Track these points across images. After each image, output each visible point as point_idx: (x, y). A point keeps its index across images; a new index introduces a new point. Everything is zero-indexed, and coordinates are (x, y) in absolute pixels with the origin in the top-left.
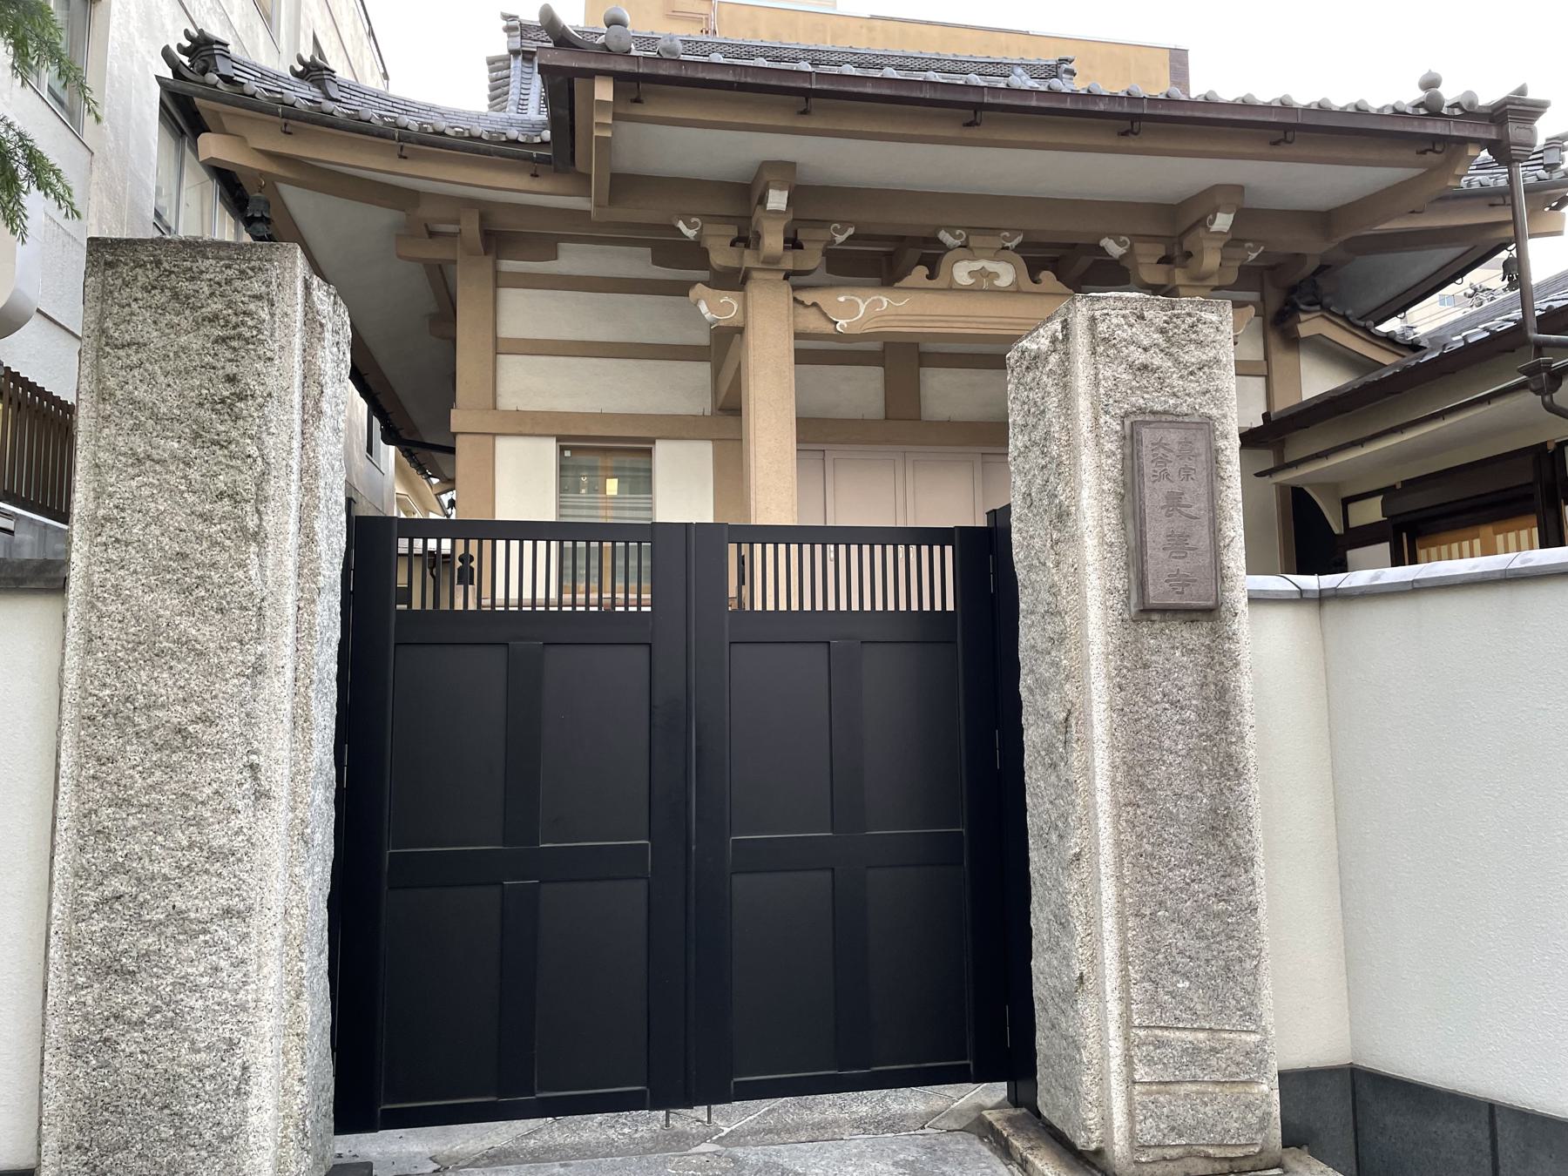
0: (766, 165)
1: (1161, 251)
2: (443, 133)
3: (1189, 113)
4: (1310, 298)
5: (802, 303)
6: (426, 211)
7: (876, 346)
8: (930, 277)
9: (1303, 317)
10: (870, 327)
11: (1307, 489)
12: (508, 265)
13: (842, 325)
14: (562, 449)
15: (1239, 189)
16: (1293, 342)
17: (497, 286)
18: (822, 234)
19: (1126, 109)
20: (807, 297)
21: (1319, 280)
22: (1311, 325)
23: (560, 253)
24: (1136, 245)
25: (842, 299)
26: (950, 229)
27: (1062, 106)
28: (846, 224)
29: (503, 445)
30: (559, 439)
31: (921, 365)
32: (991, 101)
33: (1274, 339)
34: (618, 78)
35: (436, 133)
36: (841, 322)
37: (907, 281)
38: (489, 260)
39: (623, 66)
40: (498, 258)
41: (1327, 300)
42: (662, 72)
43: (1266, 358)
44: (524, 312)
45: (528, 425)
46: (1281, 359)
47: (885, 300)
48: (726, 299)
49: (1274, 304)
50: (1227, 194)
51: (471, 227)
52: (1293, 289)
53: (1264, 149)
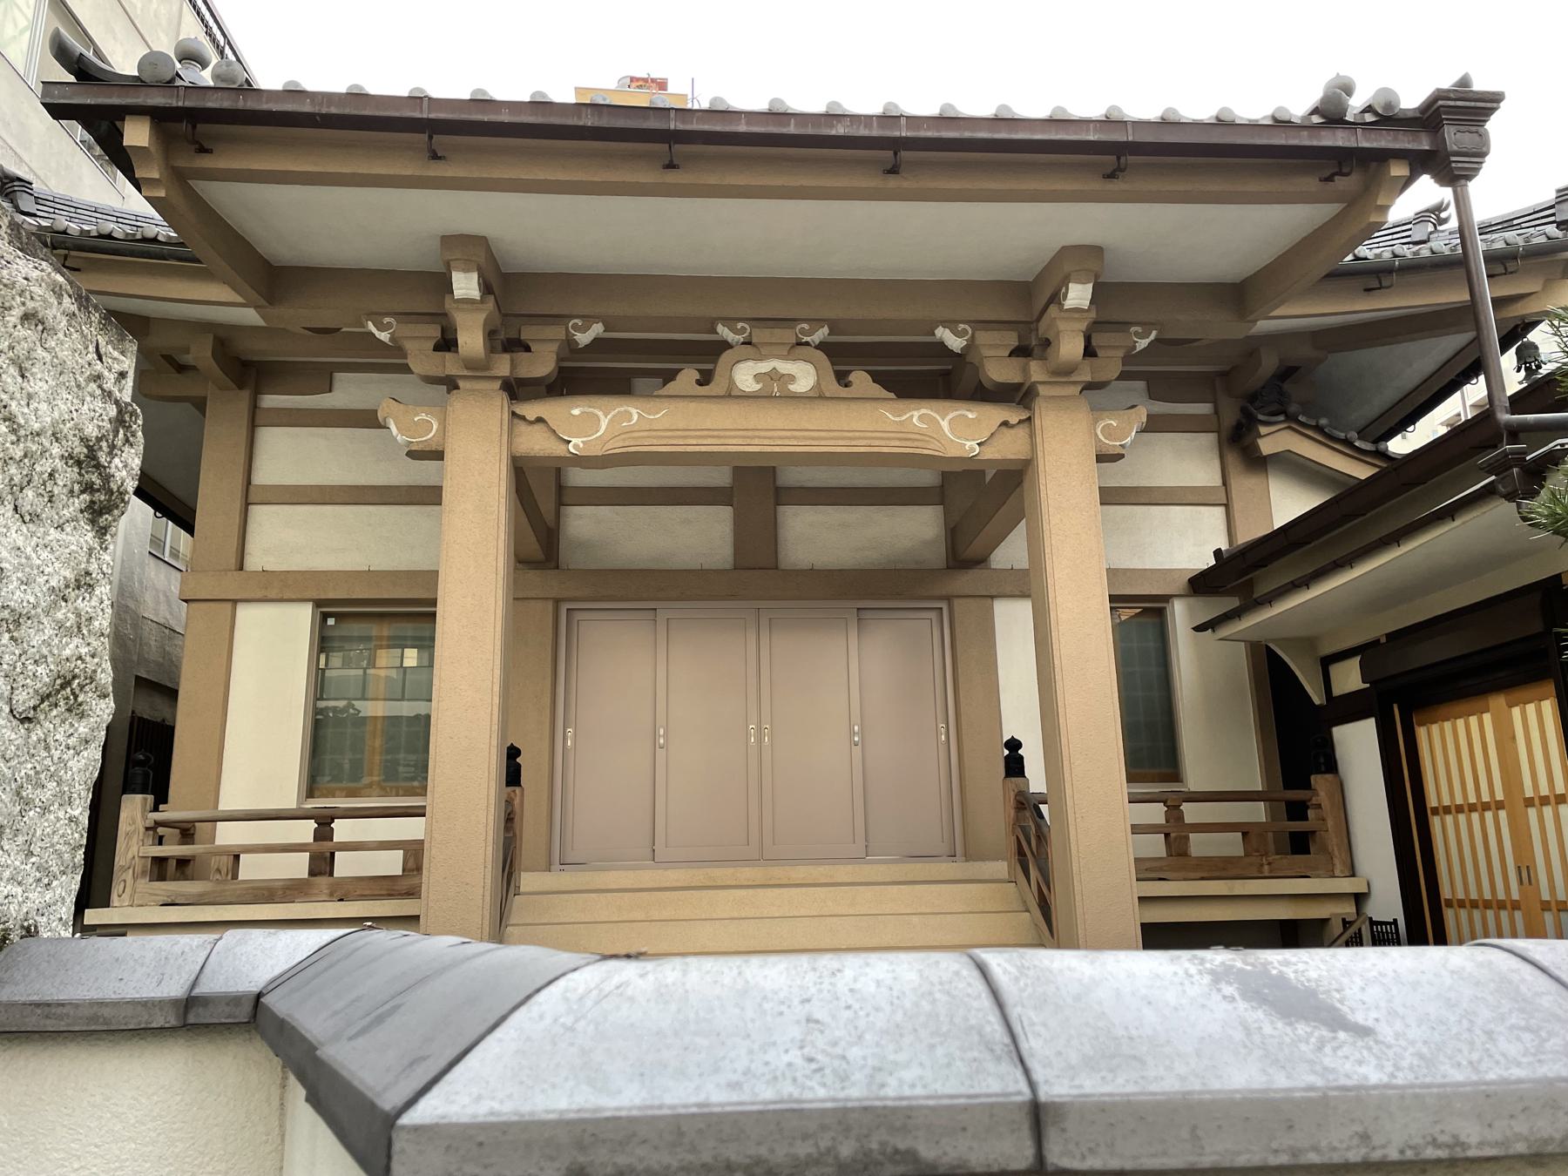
0: (452, 241)
1: (1012, 340)
2: (109, 236)
3: (967, 135)
4: (1275, 407)
5: (523, 418)
6: (159, 341)
7: (720, 477)
8: (700, 383)
9: (1263, 430)
10: (615, 447)
11: (1272, 646)
12: (270, 401)
13: (577, 445)
14: (325, 616)
15: (1096, 251)
16: (1258, 463)
17: (253, 426)
18: (557, 332)
19: (876, 132)
20: (531, 410)
21: (1287, 386)
22: (1274, 440)
23: (336, 385)
24: (978, 334)
25: (576, 412)
26: (729, 321)
27: (784, 130)
28: (589, 319)
29: (245, 614)
30: (318, 603)
31: (778, 503)
32: (681, 127)
33: (1233, 459)
34: (160, 117)
35: (101, 236)
36: (574, 441)
37: (672, 388)
38: (245, 395)
39: (157, 99)
40: (257, 393)
41: (1293, 408)
42: (210, 105)
43: (1224, 484)
44: (286, 455)
45: (279, 588)
46: (1244, 484)
47: (634, 411)
48: (424, 416)
49: (1230, 416)
50: (1082, 258)
51: (201, 353)
52: (1253, 397)
53: (1096, 185)
